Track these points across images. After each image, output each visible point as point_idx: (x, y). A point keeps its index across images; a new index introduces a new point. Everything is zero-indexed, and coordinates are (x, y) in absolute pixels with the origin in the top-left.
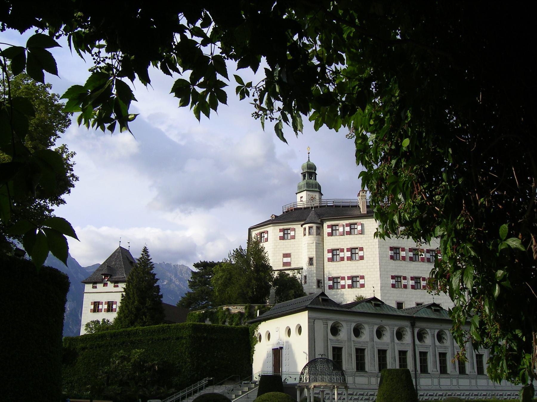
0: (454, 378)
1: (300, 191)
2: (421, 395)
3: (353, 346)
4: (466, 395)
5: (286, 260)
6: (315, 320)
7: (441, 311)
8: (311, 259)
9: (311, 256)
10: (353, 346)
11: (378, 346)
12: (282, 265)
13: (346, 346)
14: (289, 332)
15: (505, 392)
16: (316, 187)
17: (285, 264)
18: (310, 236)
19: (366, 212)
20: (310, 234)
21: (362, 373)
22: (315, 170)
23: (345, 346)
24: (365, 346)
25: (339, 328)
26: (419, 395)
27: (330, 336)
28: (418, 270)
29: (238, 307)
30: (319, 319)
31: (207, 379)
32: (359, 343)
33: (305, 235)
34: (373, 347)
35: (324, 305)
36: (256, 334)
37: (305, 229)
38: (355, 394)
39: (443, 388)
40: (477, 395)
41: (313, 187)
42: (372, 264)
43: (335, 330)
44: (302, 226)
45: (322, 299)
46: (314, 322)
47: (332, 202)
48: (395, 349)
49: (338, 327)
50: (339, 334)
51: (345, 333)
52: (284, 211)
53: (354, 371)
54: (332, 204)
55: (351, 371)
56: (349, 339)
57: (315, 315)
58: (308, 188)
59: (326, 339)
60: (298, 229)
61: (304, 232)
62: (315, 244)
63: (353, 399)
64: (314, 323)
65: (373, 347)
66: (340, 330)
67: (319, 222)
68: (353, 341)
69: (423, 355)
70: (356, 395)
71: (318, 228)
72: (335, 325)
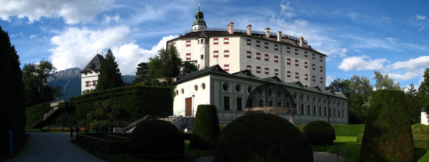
1: (195, 24)
3: (235, 97)
5: (188, 57)
6: (214, 80)
8: (202, 56)
9: (202, 54)
10: (235, 97)
12: (186, 59)
13: (232, 96)
14: (196, 88)
17: (187, 59)
18: (202, 44)
19: (233, 34)
20: (202, 43)
21: (240, 112)
23: (231, 96)
24: (243, 96)
25: (228, 86)
27: (223, 90)
28: (259, 63)
29: (163, 79)
30: (216, 80)
31: (147, 116)
32: (239, 94)
33: (199, 44)
35: (219, 72)
36: (175, 90)
37: (199, 41)
42: (236, 59)
43: (225, 87)
45: (218, 68)
46: (213, 81)
49: (227, 85)
50: (228, 90)
51: (231, 89)
53: (236, 110)
54: (213, 30)
55: (235, 110)
56: (234, 92)
57: (215, 77)
59: (220, 92)
60: (194, 42)
61: (198, 42)
62: (204, 48)
64: (213, 82)
66: (228, 87)
67: (207, 37)
68: (236, 93)
71: (206, 40)
72: (225, 84)
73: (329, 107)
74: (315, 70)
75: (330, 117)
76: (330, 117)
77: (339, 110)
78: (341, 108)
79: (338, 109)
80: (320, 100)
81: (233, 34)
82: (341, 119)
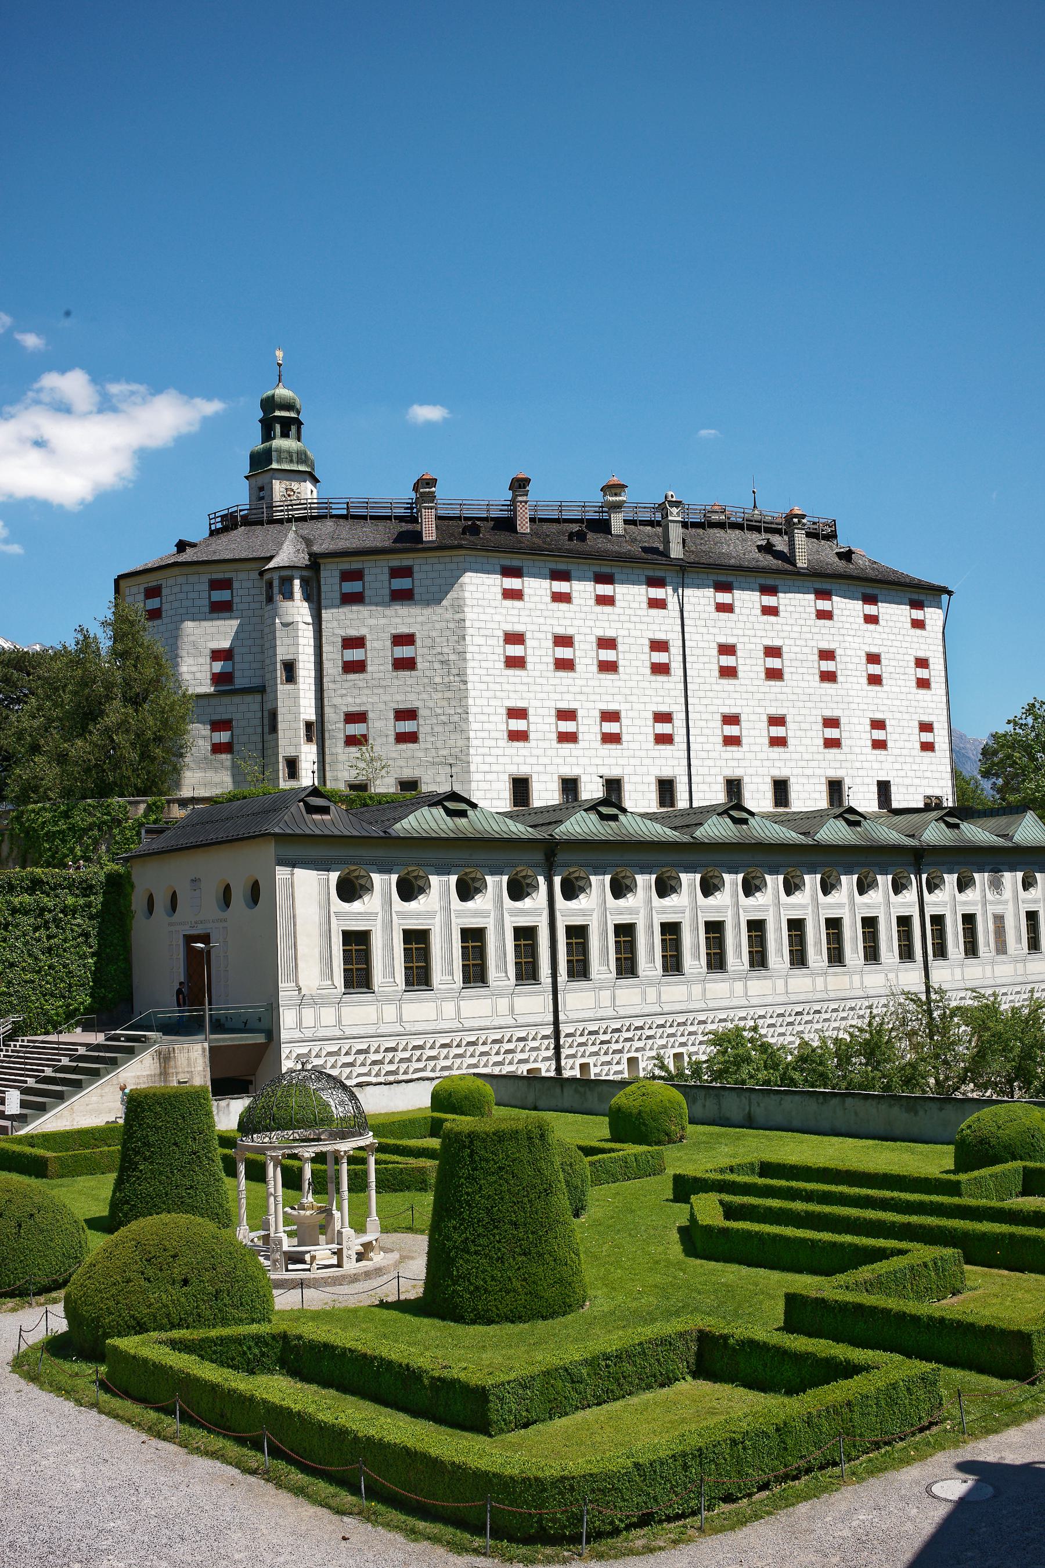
0: (651, 985)
2: (568, 1035)
4: (679, 1024)
7: (622, 817)
11: (459, 921)
15: (770, 1010)
16: (300, 461)
19: (434, 538)
22: (298, 413)
26: (563, 1035)
27: (338, 905)
34: (449, 924)
37: (270, 585)
38: (401, 1047)
39: (622, 1012)
40: (704, 1022)
41: (291, 461)
44: (261, 574)
47: (345, 506)
48: (503, 925)
52: (213, 527)
54: (344, 512)
58: (279, 462)
61: (267, 591)
63: (397, 1059)
65: (449, 924)
69: (578, 934)
70: (405, 1049)
71: (305, 583)
73: (926, 909)
74: (885, 688)
75: (934, 964)
76: (933, 964)
77: (999, 920)
78: (1010, 906)
79: (991, 909)
80: (869, 879)
81: (434, 538)
82: (1020, 966)
